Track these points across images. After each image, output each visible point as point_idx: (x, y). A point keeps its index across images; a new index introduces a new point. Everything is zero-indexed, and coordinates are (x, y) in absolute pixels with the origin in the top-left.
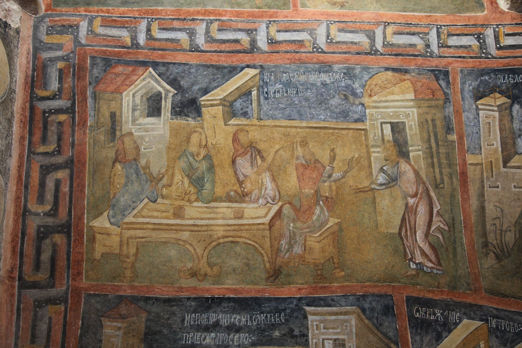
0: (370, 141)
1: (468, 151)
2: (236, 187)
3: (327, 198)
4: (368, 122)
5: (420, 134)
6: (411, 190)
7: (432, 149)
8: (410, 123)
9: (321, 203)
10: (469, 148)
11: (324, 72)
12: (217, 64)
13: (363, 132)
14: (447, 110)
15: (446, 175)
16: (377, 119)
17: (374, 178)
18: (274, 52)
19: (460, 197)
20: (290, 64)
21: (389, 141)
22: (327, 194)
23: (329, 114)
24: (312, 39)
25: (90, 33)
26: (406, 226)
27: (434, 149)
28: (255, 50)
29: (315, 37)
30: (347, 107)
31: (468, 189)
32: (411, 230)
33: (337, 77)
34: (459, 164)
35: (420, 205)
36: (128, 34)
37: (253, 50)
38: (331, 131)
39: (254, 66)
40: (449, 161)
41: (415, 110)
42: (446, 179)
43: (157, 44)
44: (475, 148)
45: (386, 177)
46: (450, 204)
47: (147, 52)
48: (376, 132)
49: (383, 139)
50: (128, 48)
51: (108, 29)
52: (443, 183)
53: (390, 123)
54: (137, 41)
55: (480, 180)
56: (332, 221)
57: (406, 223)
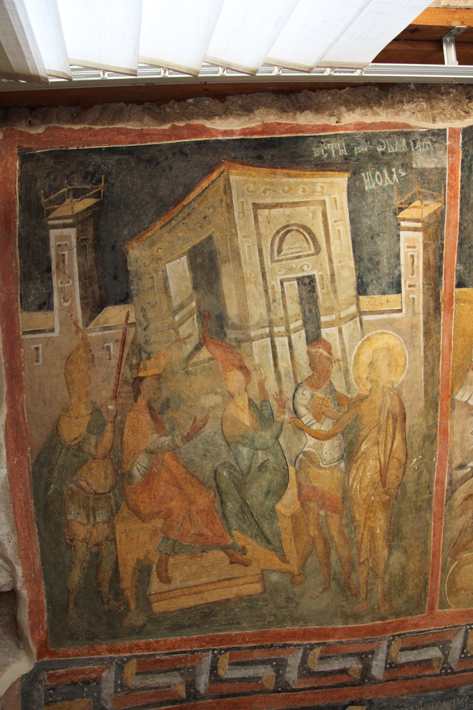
11: (447, 700)
12: (312, 705)
18: (391, 680)
20: (407, 695)
24: (443, 656)
25: (119, 690)
28: (367, 681)
29: (447, 652)
33: (461, 702)
36: (182, 680)
37: (364, 680)
39: (360, 702)
43: (225, 688)
47: (210, 703)
50: (182, 701)
51: (149, 676)
54: (195, 688)
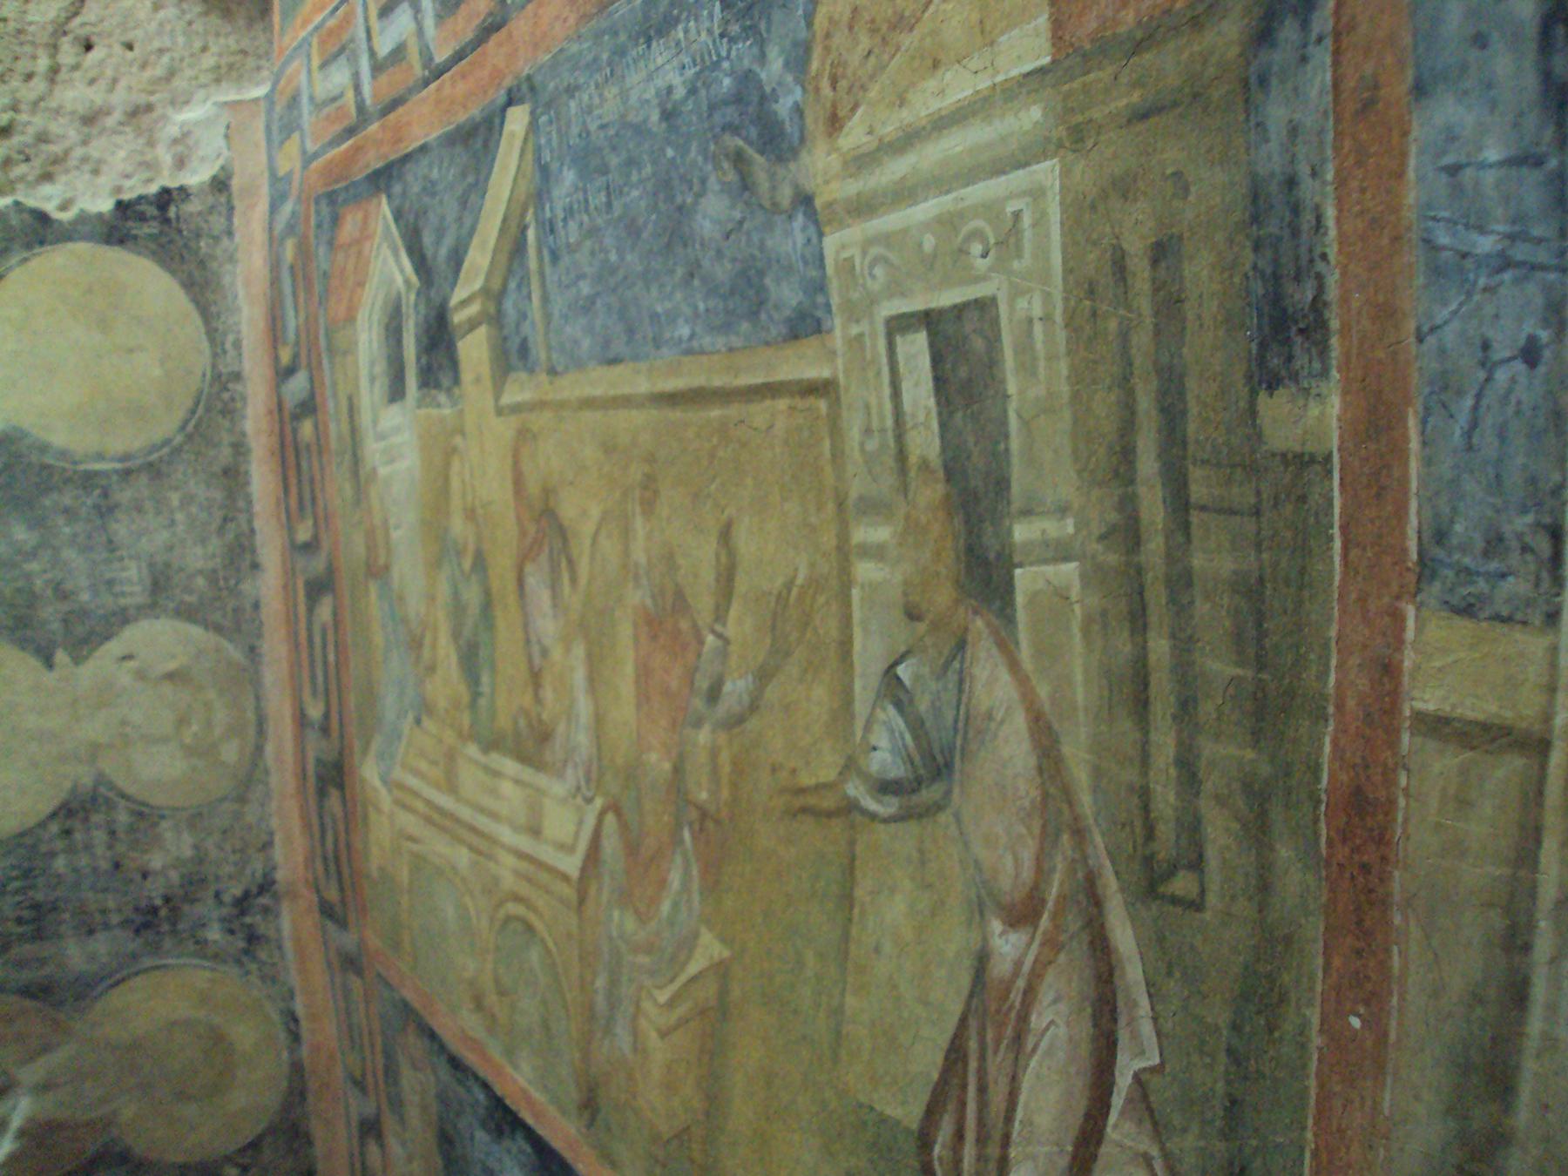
0: (850, 469)
1: (1427, 569)
2: (527, 700)
3: (704, 814)
4: (838, 322)
5: (1076, 396)
6: (1009, 862)
7: (1138, 544)
8: (1022, 303)
9: (687, 835)
10: (1441, 536)
13: (822, 405)
14: (1277, 114)
15: (1221, 801)
16: (873, 301)
17: (859, 733)
19: (1314, 1016)
21: (925, 465)
22: (704, 796)
23: (701, 306)
26: (963, 1104)
27: (1154, 546)
30: (755, 238)
31: (1384, 966)
32: (982, 1140)
34: (1340, 707)
35: (1046, 995)
38: (715, 413)
40: (1261, 666)
41: (1047, 172)
42: (1219, 833)
44: (1494, 543)
45: (908, 738)
46: (1230, 1051)
48: (873, 402)
49: (902, 455)
52: (1197, 864)
53: (928, 319)
55: (1498, 921)
56: (709, 948)
57: (964, 1087)
